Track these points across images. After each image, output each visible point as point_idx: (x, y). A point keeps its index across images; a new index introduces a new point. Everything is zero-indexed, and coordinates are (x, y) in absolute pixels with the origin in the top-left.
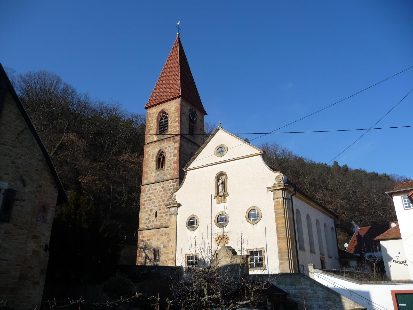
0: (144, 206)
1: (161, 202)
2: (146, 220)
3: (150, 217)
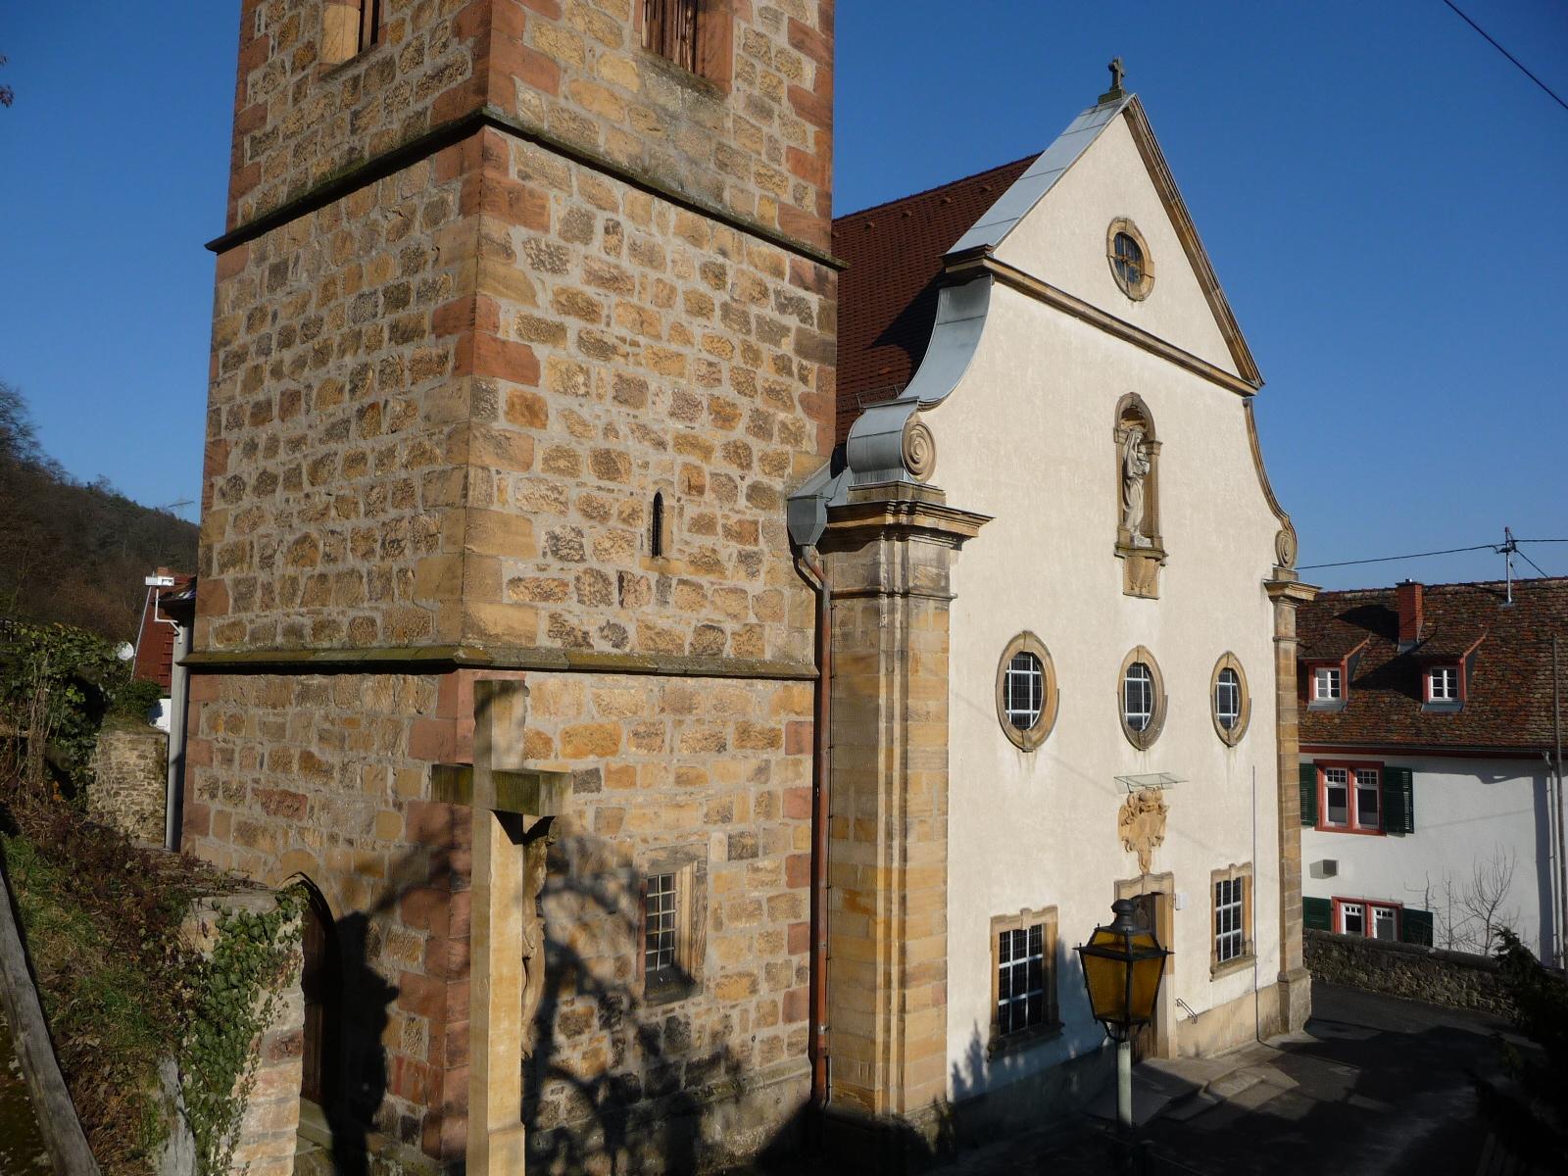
0: (528, 390)
1: (705, 417)
2: (555, 565)
3: (594, 534)
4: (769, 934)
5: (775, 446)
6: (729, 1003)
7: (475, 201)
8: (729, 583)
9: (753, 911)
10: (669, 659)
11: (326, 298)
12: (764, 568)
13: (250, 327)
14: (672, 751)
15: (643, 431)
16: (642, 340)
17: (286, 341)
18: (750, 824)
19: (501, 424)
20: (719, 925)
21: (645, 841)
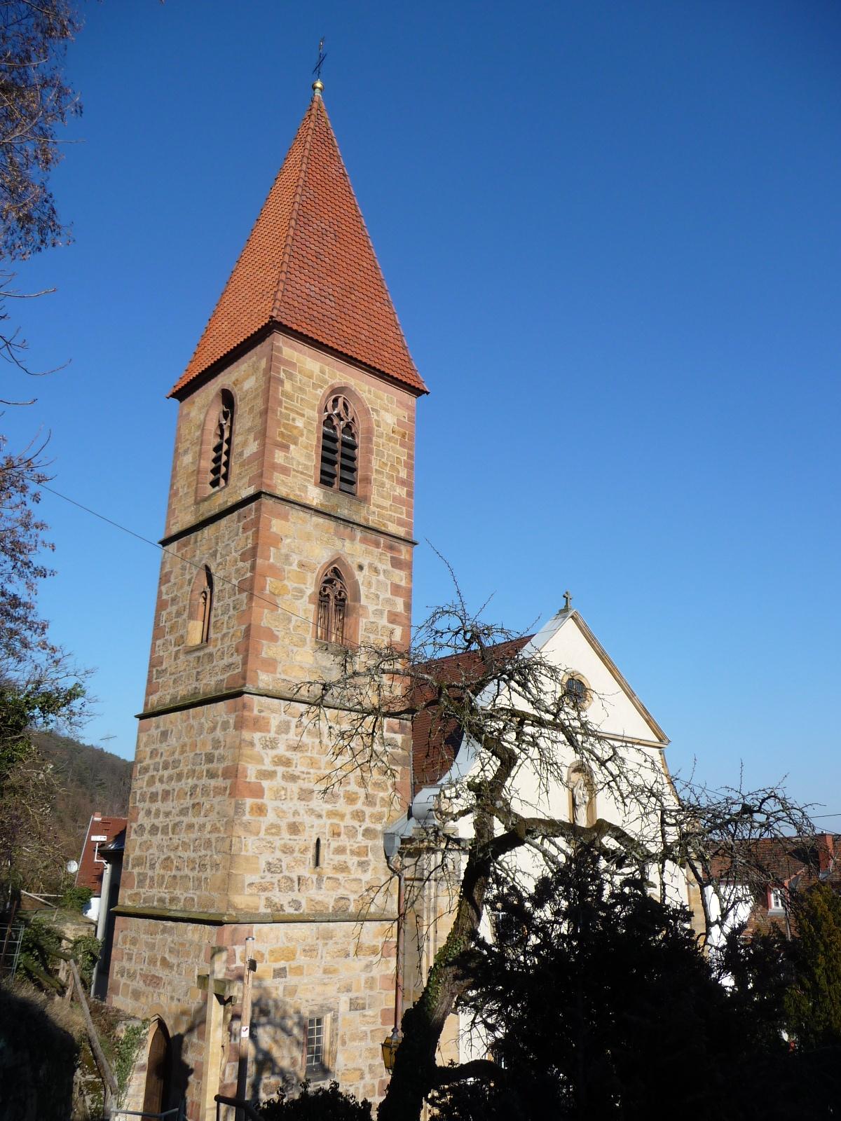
0: (259, 801)
1: (342, 801)
2: (268, 875)
3: (286, 860)
4: (371, 1049)
5: (378, 809)
6: (349, 1084)
7: (239, 725)
8: (352, 877)
9: (363, 1037)
10: (321, 914)
11: (182, 752)
12: (371, 868)
13: (151, 757)
14: (322, 958)
15: (311, 811)
16: (312, 771)
17: (166, 767)
18: (362, 993)
19: (247, 817)
20: (344, 1043)
21: (307, 1001)
